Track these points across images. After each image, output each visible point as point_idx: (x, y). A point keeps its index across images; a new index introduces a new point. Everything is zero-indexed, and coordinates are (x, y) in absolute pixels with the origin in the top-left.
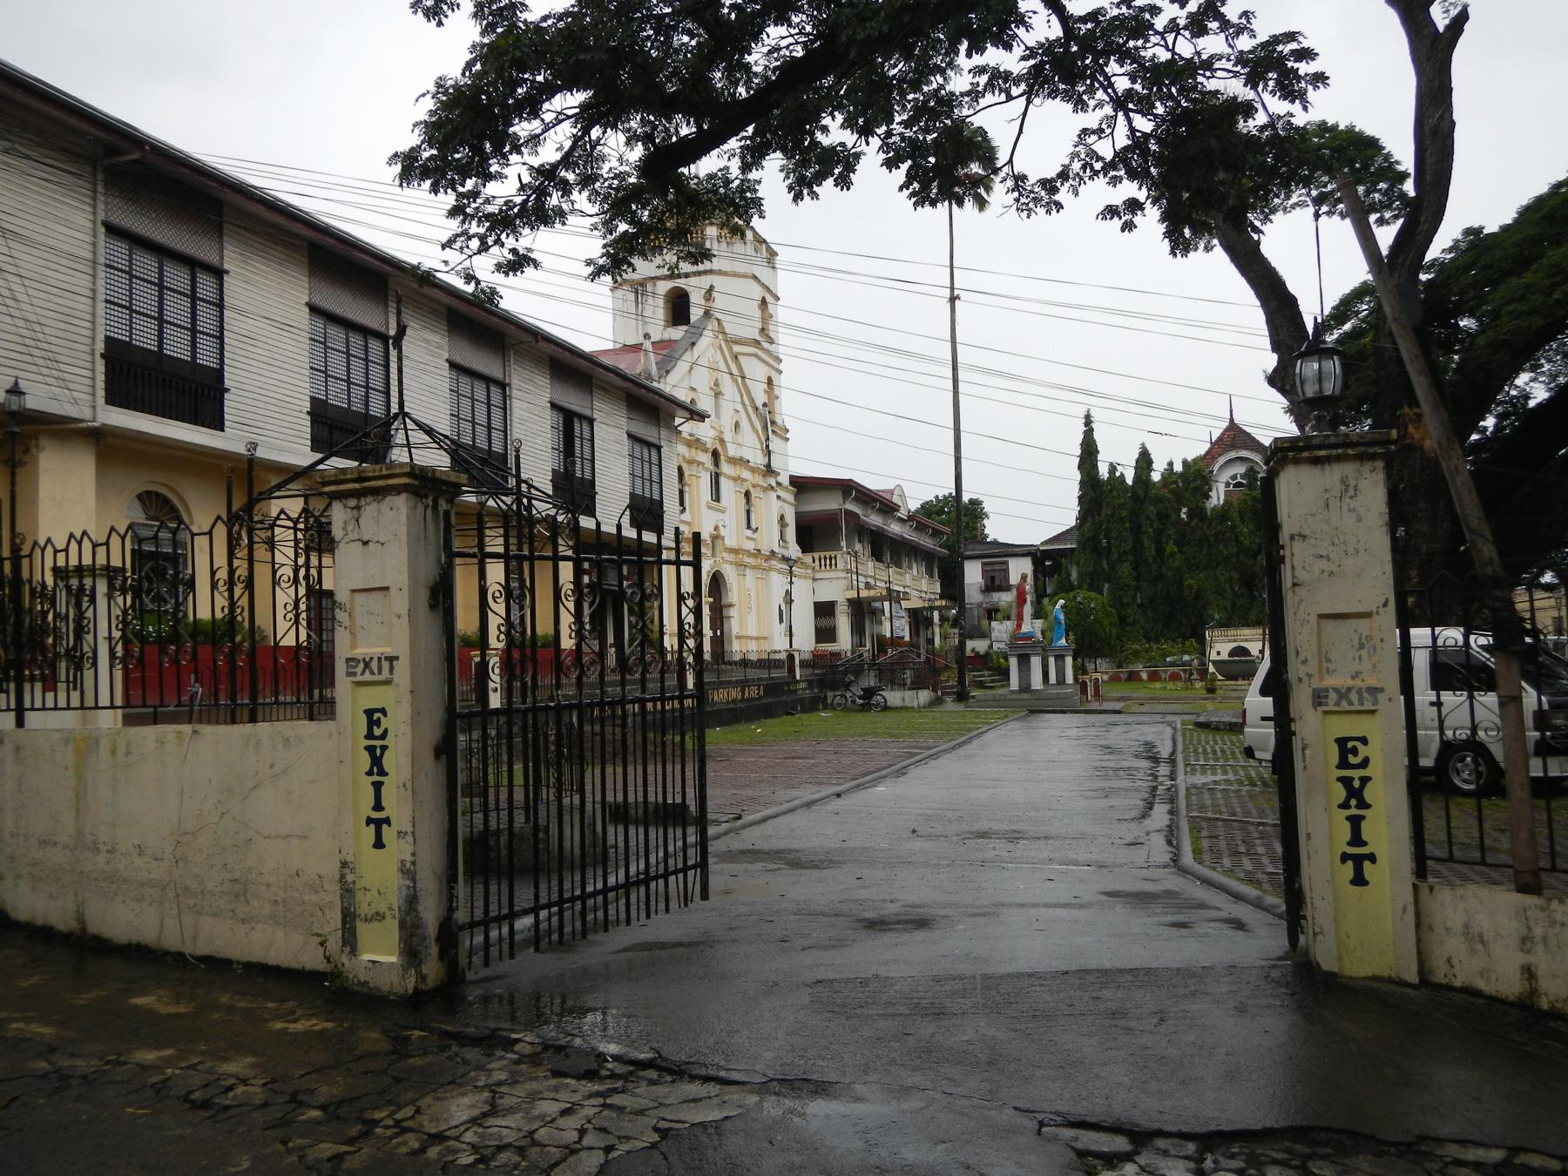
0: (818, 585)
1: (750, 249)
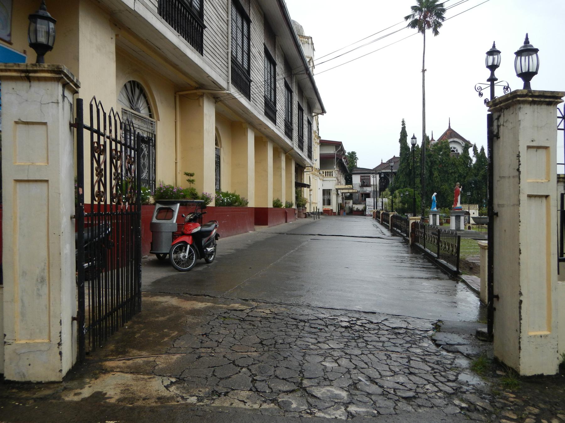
0: (325, 183)
1: (310, 45)
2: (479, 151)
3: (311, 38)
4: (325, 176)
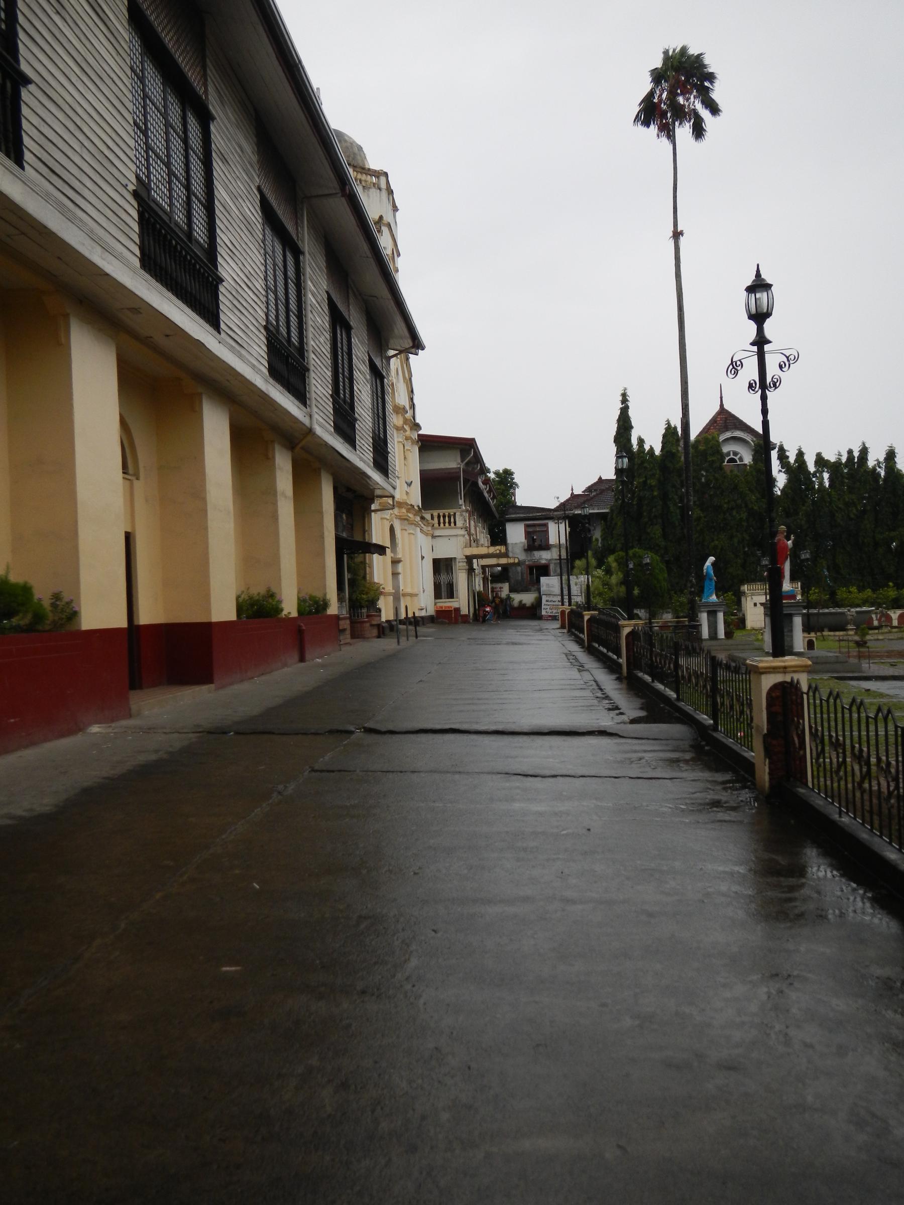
0: (439, 542)
2: (792, 459)
3: (386, 174)
4: (436, 525)
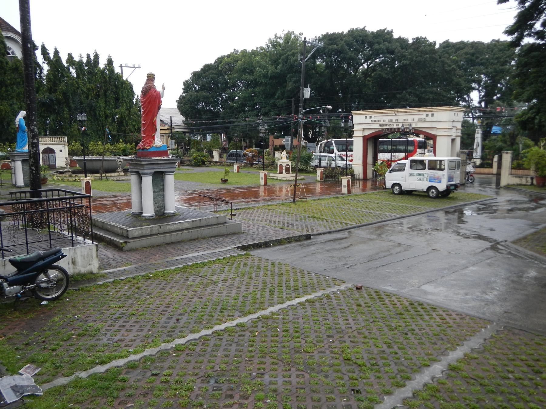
2: (51, 55)
